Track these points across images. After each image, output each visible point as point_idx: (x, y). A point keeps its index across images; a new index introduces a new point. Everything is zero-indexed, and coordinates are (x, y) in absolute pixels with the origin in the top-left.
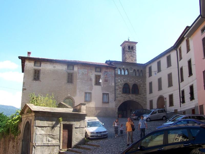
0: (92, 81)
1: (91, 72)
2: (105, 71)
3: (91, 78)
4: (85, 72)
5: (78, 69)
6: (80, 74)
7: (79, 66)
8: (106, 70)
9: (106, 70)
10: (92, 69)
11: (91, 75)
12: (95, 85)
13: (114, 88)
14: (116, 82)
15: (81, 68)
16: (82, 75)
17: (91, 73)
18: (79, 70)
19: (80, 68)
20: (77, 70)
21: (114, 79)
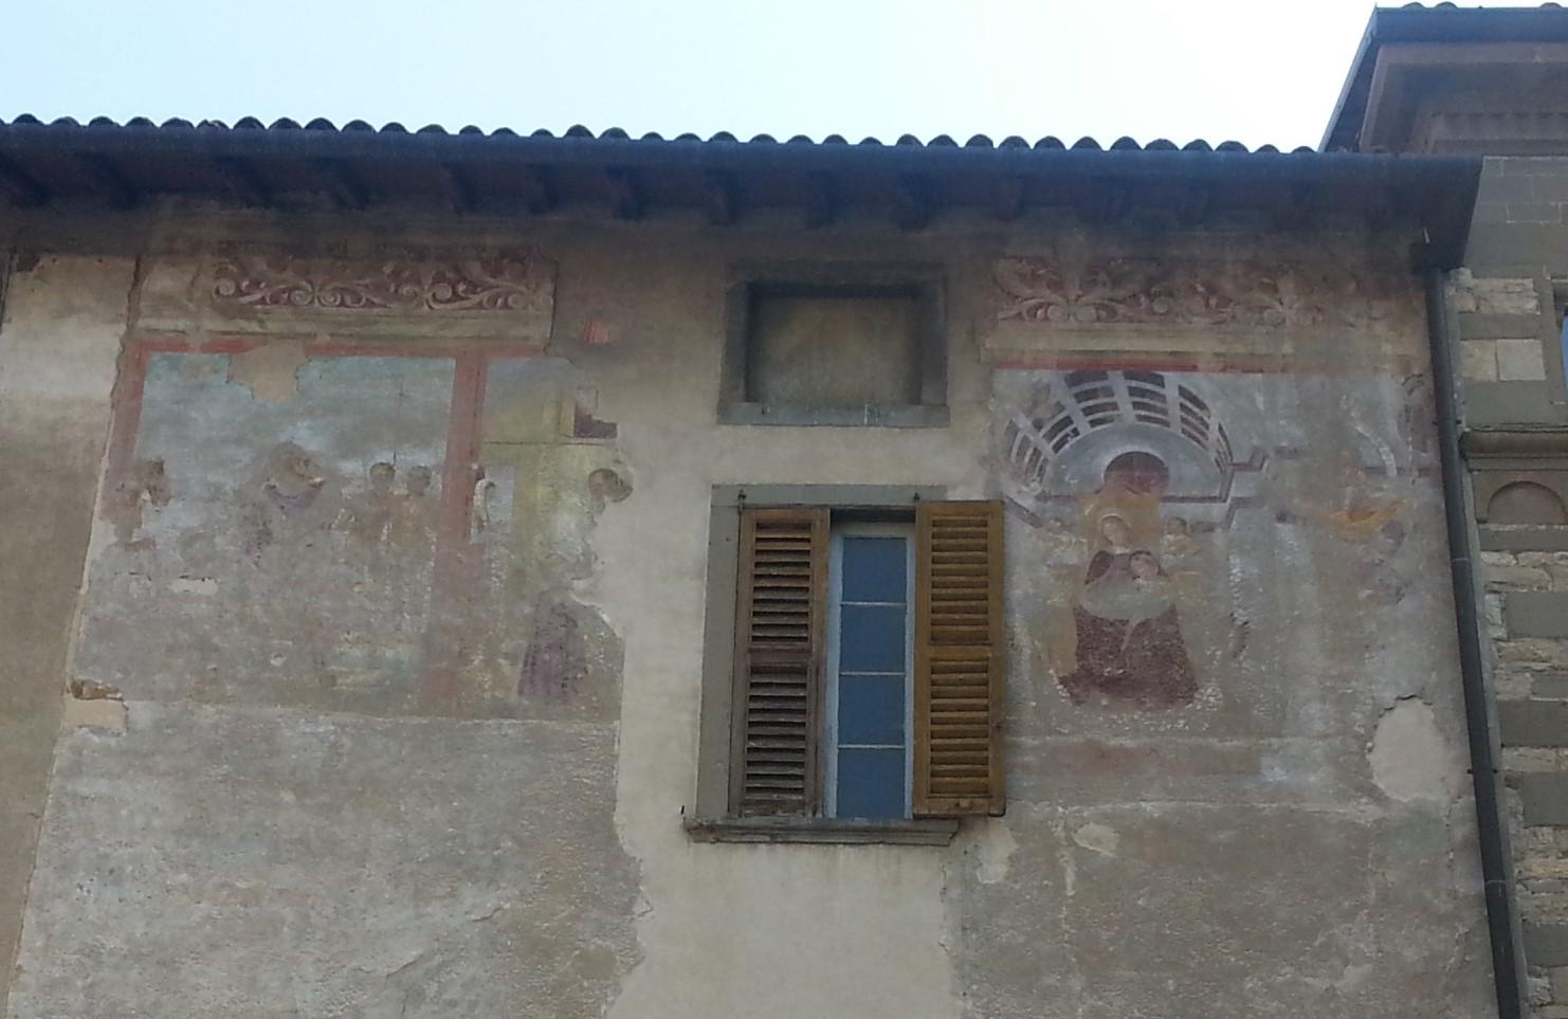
0: (608, 709)
1: (586, 428)
2: (1085, 375)
3: (578, 592)
4: (349, 446)
5: (134, 361)
6: (166, 523)
7: (162, 281)
8: (1107, 311)
9: (1128, 342)
10: (602, 334)
11: (565, 524)
12: (700, 830)
13: (1469, 884)
14: (1506, 686)
15: (232, 346)
16: (265, 536)
17: (584, 457)
18: (158, 389)
19: (213, 324)
20: (100, 384)
21: (1426, 602)
